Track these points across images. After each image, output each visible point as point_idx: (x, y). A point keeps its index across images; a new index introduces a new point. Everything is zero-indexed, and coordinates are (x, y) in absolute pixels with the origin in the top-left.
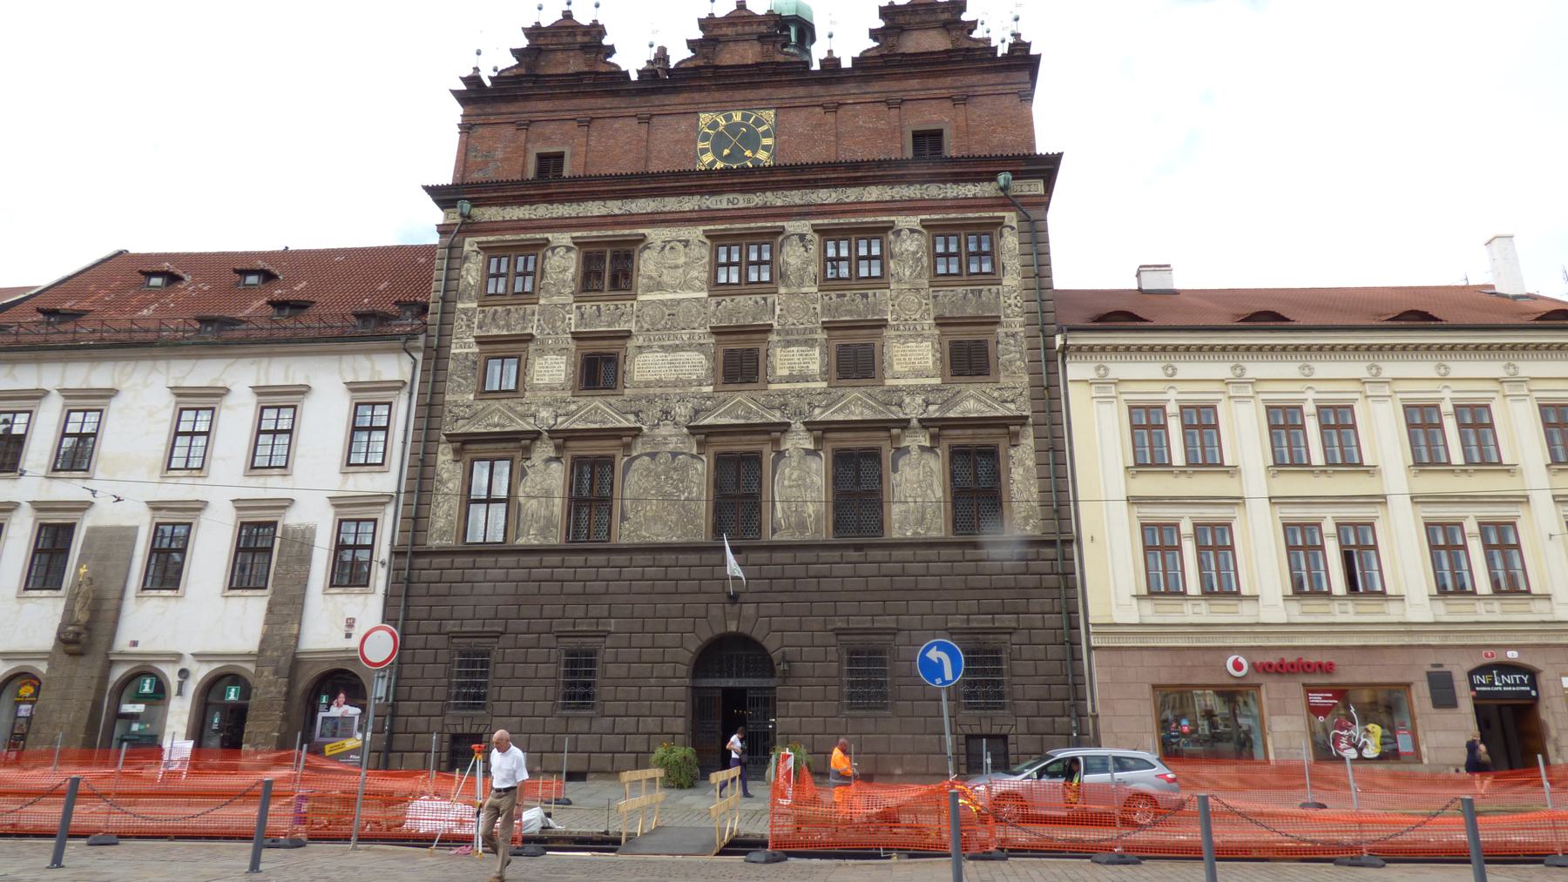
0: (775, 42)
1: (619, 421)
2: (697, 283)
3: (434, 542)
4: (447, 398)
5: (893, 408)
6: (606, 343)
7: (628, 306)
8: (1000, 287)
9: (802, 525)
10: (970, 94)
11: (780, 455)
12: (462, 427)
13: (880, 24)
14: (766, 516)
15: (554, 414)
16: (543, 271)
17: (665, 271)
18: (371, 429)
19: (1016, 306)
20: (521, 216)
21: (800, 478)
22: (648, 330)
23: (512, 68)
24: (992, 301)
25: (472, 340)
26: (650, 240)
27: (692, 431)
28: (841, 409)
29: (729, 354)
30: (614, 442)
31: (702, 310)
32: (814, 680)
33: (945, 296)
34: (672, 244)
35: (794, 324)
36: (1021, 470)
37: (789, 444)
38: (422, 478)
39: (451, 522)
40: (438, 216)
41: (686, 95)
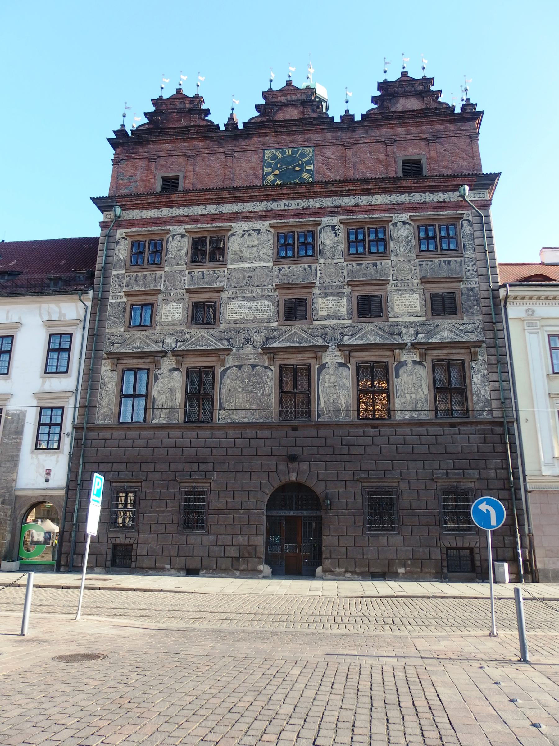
0: (312, 105)
1: (217, 345)
2: (266, 257)
3: (100, 422)
4: (107, 330)
5: (395, 336)
6: (208, 295)
7: (222, 271)
9: (337, 411)
10: (438, 136)
12: (117, 349)
13: (379, 94)
14: (314, 405)
16: (167, 250)
18: (59, 350)
19: (473, 270)
20: (153, 216)
21: (335, 381)
22: (235, 287)
23: (145, 124)
24: (458, 268)
25: (122, 294)
27: (265, 351)
28: (361, 337)
29: (288, 302)
30: (214, 359)
31: (270, 274)
34: (249, 232)
35: (329, 283)
36: (479, 376)
40: (100, 217)
41: (256, 139)
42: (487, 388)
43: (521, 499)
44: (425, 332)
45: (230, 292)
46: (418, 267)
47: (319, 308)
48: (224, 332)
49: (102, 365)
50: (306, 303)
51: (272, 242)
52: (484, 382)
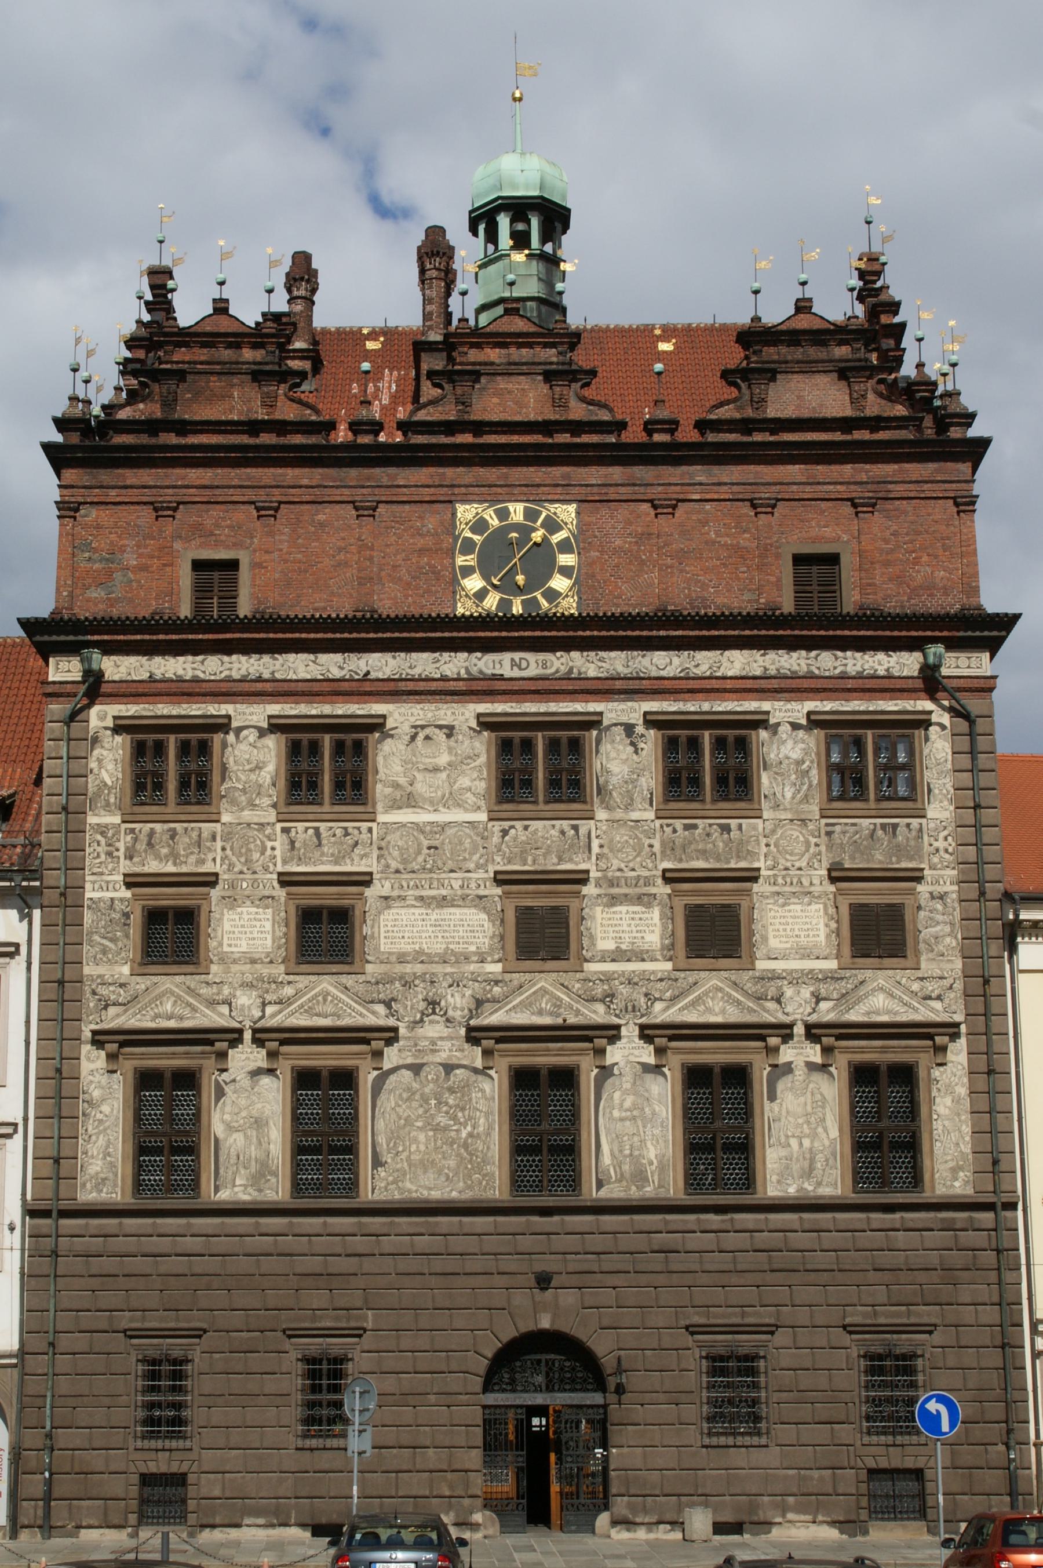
1: (361, 1015)
2: (470, 798)
3: (87, 1195)
4: (87, 970)
5: (771, 1005)
7: (364, 830)
8: (923, 821)
9: (640, 1177)
11: (606, 1072)
12: (115, 1019)
15: (259, 1001)
16: (224, 768)
17: (419, 776)
19: (946, 851)
20: (180, 672)
21: (635, 1106)
22: (397, 871)
24: (912, 843)
26: (390, 724)
28: (694, 1004)
29: (525, 915)
32: (662, 1397)
33: (844, 833)
34: (427, 731)
35: (620, 870)
36: (948, 1101)
37: (615, 1054)
38: (59, 1096)
39: (112, 1165)
42: (964, 1127)
43: (1024, 1368)
44: (835, 996)
45: (387, 884)
46: (824, 839)
47: (598, 932)
48: (377, 983)
49: (82, 1057)
50: (567, 918)
51: (483, 759)
52: (959, 1115)
